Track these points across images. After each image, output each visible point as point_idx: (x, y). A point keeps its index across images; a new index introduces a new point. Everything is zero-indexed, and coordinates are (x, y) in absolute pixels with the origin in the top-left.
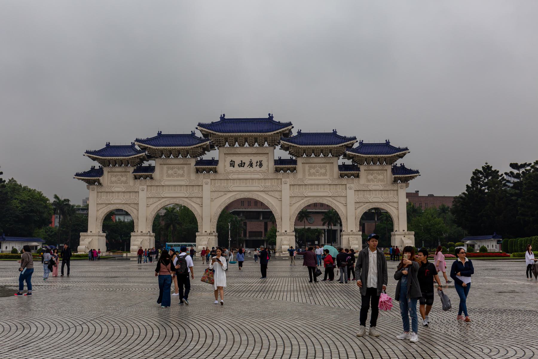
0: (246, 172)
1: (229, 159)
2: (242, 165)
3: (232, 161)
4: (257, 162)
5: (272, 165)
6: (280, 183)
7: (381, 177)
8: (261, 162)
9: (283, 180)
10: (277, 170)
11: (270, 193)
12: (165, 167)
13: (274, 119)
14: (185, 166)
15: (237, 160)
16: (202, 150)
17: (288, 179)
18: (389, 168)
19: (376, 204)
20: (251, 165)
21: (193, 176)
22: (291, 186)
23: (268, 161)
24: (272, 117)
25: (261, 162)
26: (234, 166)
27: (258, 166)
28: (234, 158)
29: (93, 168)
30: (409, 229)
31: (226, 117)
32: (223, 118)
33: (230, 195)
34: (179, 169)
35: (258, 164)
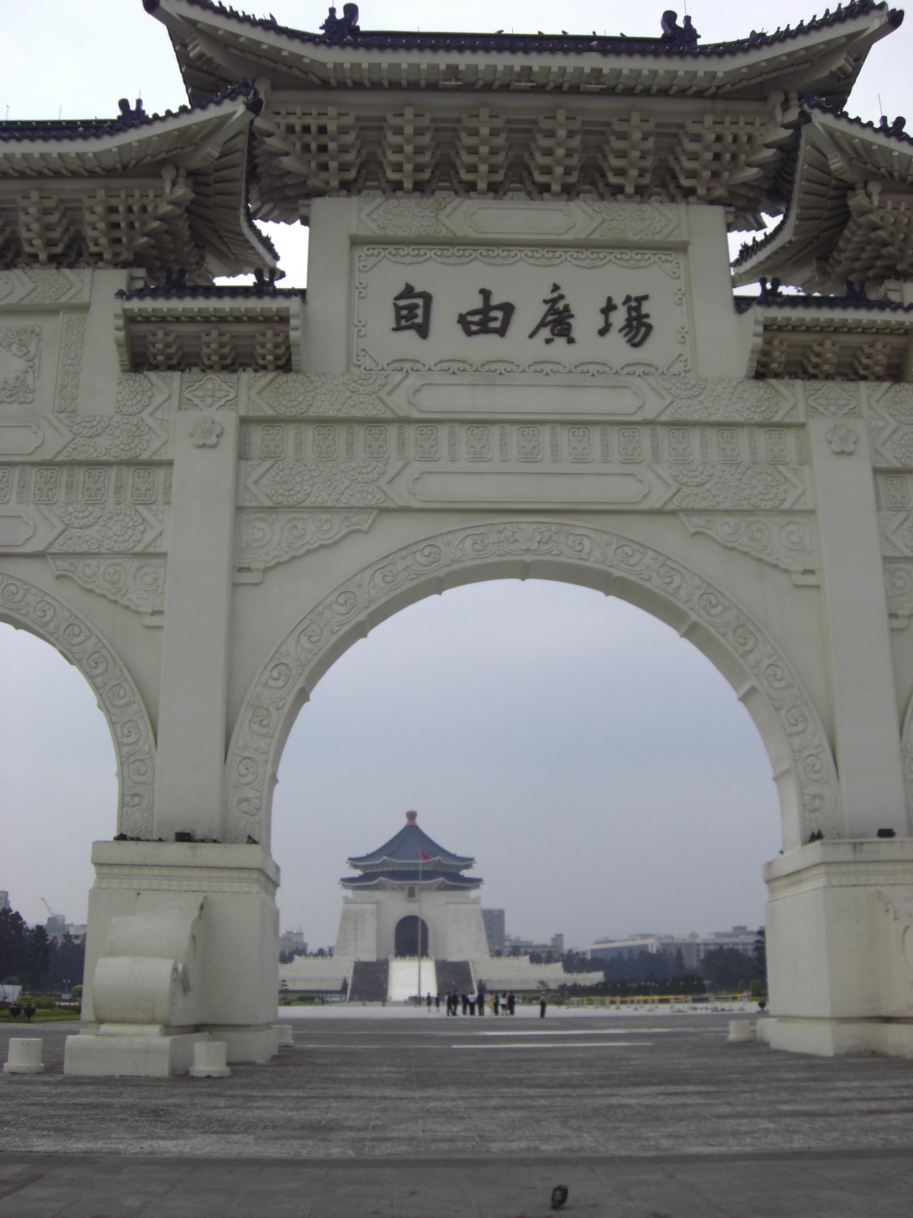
0: (524, 376)
1: (388, 277)
2: (488, 318)
3: (409, 292)
4: (609, 308)
8: (635, 304)
9: (818, 428)
10: (761, 373)
11: (722, 528)
15: (453, 288)
16: (182, 191)
20: (558, 321)
25: (635, 304)
26: (423, 331)
28: (428, 274)
31: (365, 23)
35: (619, 318)
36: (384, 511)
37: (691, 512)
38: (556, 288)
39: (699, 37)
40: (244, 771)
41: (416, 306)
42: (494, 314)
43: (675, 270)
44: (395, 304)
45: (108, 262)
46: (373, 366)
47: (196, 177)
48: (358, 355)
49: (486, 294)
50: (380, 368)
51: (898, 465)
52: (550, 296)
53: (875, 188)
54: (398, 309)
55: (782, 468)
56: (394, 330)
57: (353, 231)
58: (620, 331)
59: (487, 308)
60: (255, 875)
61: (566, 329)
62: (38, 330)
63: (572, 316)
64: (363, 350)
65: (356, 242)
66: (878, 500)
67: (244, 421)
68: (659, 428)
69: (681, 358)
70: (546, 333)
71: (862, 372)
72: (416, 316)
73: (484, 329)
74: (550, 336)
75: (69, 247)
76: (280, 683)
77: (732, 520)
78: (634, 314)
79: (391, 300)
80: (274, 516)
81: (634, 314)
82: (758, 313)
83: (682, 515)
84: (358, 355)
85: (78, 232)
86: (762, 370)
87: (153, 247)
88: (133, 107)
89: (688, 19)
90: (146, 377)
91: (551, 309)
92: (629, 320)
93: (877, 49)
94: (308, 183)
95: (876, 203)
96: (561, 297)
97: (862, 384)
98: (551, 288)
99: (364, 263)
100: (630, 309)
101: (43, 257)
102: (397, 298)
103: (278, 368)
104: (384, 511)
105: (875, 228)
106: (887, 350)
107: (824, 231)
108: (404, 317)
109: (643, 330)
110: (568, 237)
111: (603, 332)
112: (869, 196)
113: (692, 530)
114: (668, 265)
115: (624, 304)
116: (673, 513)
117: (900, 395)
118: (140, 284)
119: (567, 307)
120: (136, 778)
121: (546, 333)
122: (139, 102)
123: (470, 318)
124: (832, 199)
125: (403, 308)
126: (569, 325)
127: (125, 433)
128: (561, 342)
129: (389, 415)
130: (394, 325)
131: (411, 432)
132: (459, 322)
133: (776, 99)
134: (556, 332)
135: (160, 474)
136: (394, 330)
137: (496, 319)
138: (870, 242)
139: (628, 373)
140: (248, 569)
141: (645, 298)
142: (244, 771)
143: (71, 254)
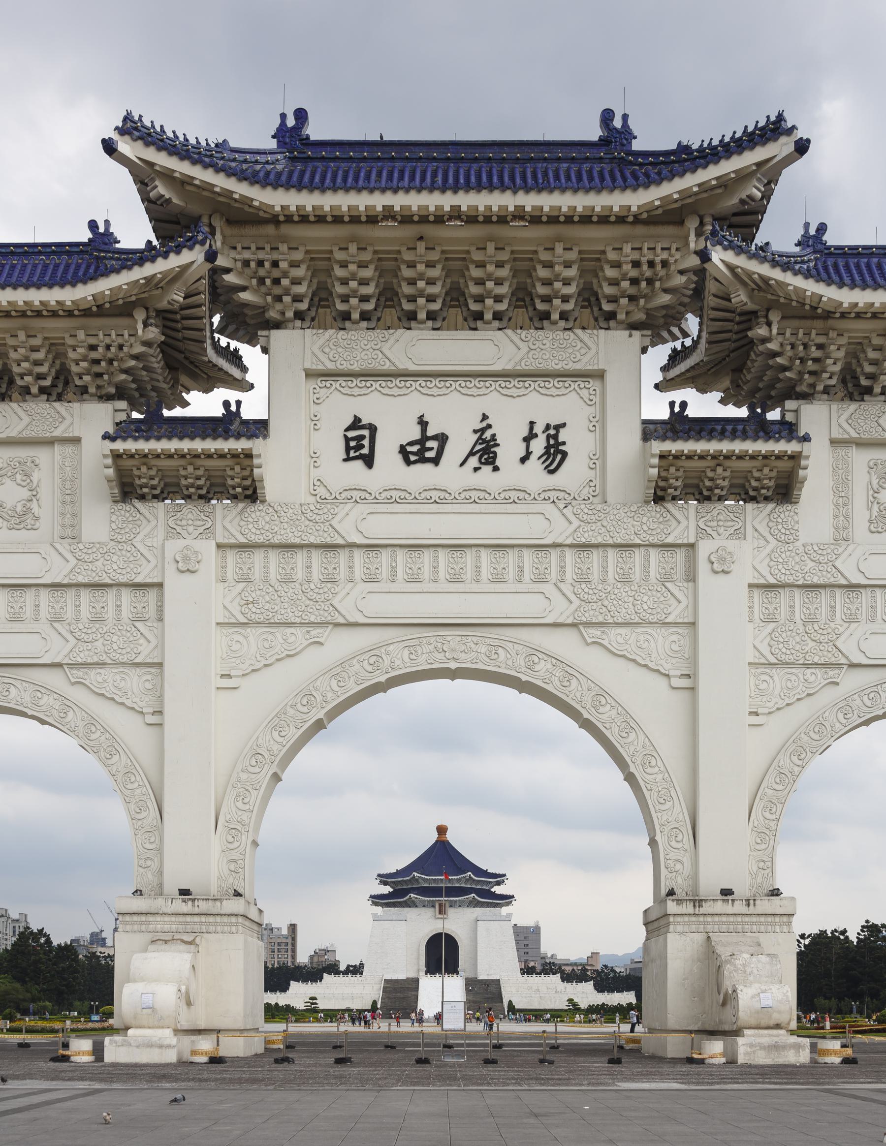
2: (424, 449)
3: (356, 424)
5: (624, 444)
6: (680, 572)
8: (554, 431)
11: (614, 637)
13: (636, 146)
14: (42, 455)
17: (742, 543)
20: (486, 451)
21: (100, 518)
22: (756, 593)
23: (599, 425)
24: (626, 134)
25: (554, 431)
26: (369, 461)
27: (535, 465)
28: (372, 405)
32: (292, 135)
35: (538, 446)
36: (337, 625)
37: (589, 624)
38: (485, 417)
39: (635, 138)
40: (230, 839)
41: (362, 437)
42: (429, 444)
43: (591, 397)
44: (345, 435)
45: (92, 395)
46: (327, 495)
47: (166, 318)
48: (314, 485)
49: (423, 424)
50: (333, 497)
51: (772, 581)
52: (480, 426)
53: (774, 317)
54: (347, 440)
55: (668, 584)
56: (344, 460)
57: (308, 365)
58: (539, 458)
59: (424, 438)
60: (240, 919)
61: (492, 457)
62: (37, 462)
63: (498, 445)
64: (319, 480)
65: (310, 374)
66: (751, 612)
67: (219, 546)
68: (567, 549)
69: (592, 484)
70: (474, 461)
71: (752, 493)
72: (363, 446)
73: (423, 460)
74: (477, 465)
75: (56, 378)
76: (257, 770)
77: (622, 631)
78: (552, 442)
79: (342, 433)
80: (249, 630)
81: (552, 442)
82: (657, 447)
83: (581, 627)
84: (314, 485)
85: (63, 365)
86: (659, 493)
87: (133, 381)
88: (102, 230)
89: (625, 117)
90: (135, 507)
91: (480, 438)
92: (548, 447)
93: (788, 175)
94: (267, 315)
95: (775, 332)
96: (489, 426)
97: (750, 506)
98: (481, 418)
99: (317, 395)
100: (549, 437)
101: (34, 390)
102: (347, 430)
103: (246, 497)
104: (337, 625)
105: (774, 354)
106: (774, 474)
107: (733, 351)
108: (353, 448)
109: (559, 457)
110: (498, 367)
111: (523, 460)
112: (769, 324)
113: (589, 640)
114: (585, 392)
115: (543, 432)
116: (574, 625)
117: (782, 516)
118: (122, 417)
119: (494, 435)
120: (148, 846)
121: (474, 461)
122: (107, 222)
123: (409, 449)
124: (738, 323)
125: (353, 439)
126: (495, 453)
127: (121, 559)
128: (487, 469)
129: (340, 541)
130: (345, 457)
131: (357, 554)
132: (400, 452)
133: (692, 224)
134: (483, 460)
135: (152, 594)
136: (344, 460)
137: (432, 449)
138: (772, 367)
139: (545, 499)
140: (229, 676)
141: (564, 425)
142: (230, 839)
143: (60, 386)
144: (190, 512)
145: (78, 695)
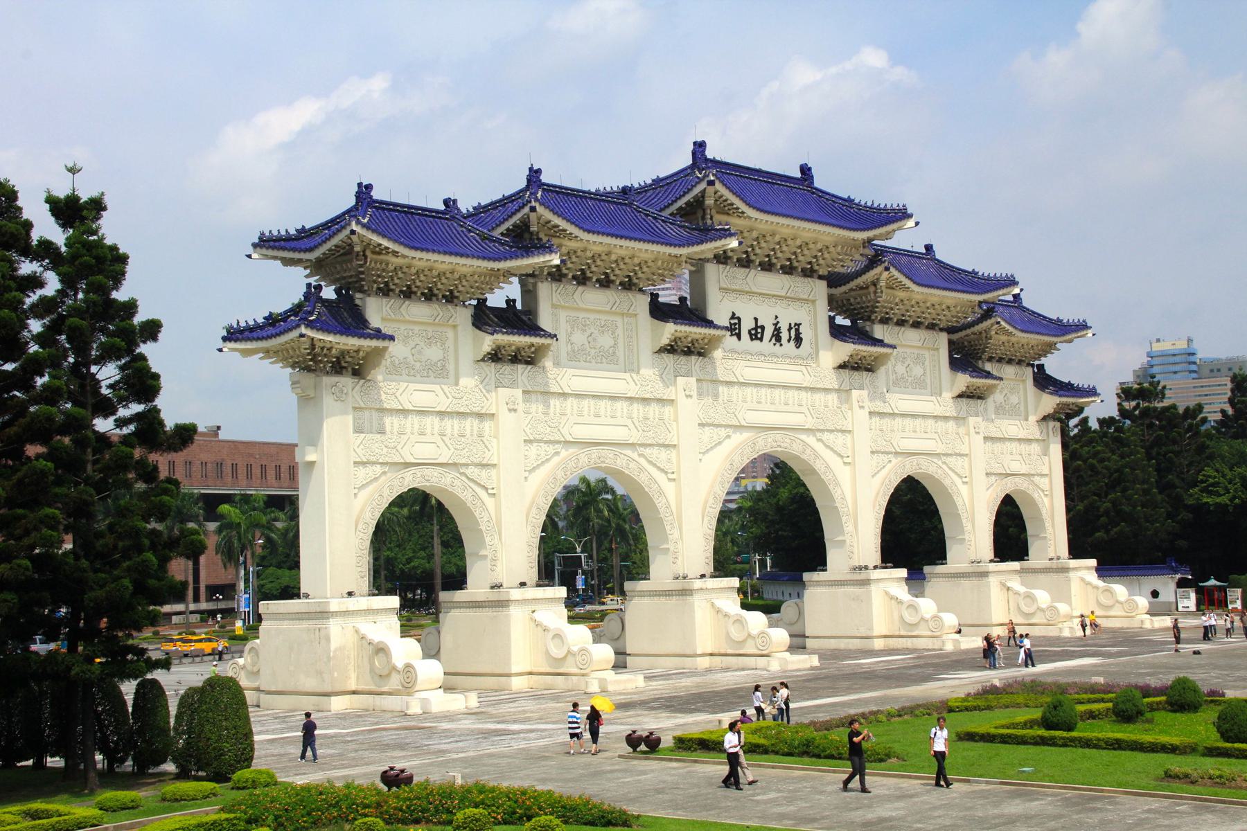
2: (757, 333)
3: (733, 316)
4: (789, 330)
7: (1014, 399)
9: (855, 393)
12: (563, 315)
13: (817, 184)
18: (1029, 372)
19: (1017, 479)
20: (777, 336)
26: (739, 339)
27: (792, 342)
29: (312, 294)
30: (1076, 551)
31: (710, 154)
33: (739, 438)
34: (603, 328)
49: (756, 319)
73: (757, 338)
144: (683, 359)
145: (642, 461)
